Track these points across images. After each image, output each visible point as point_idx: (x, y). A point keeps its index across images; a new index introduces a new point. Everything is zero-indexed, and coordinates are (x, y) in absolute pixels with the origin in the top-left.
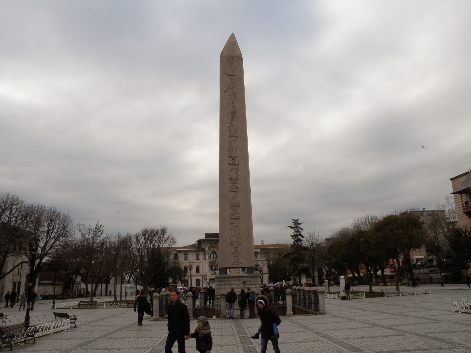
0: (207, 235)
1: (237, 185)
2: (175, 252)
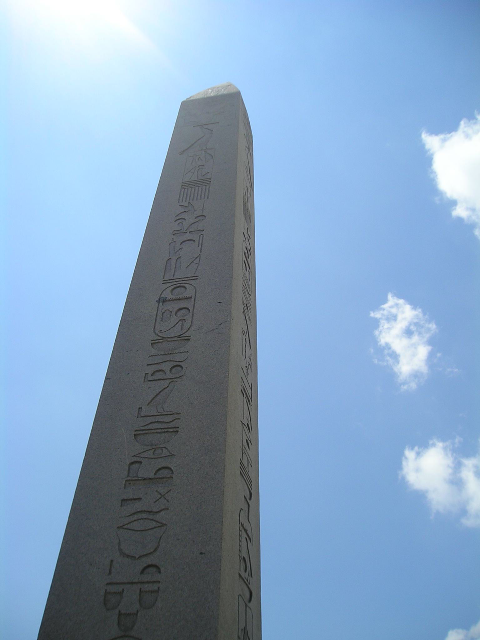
1: (178, 358)
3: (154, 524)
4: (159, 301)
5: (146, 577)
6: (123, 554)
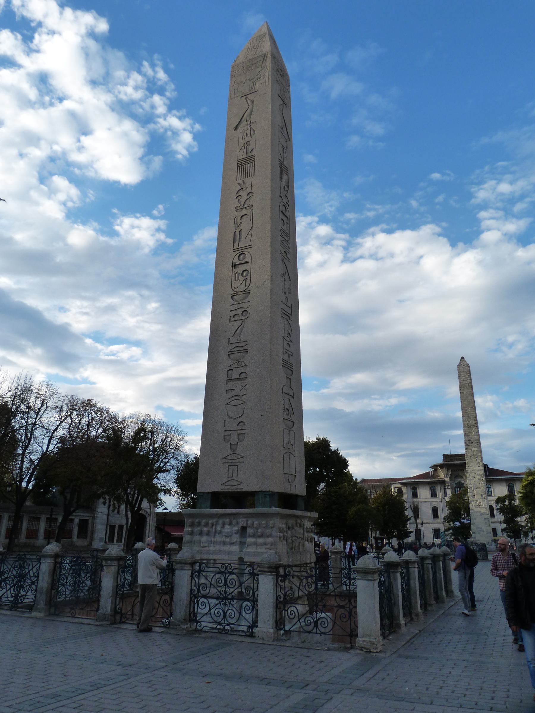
0: (446, 457)
1: (245, 305)
2: (399, 486)
3: (241, 402)
4: (232, 266)
5: (239, 428)
6: (229, 417)
